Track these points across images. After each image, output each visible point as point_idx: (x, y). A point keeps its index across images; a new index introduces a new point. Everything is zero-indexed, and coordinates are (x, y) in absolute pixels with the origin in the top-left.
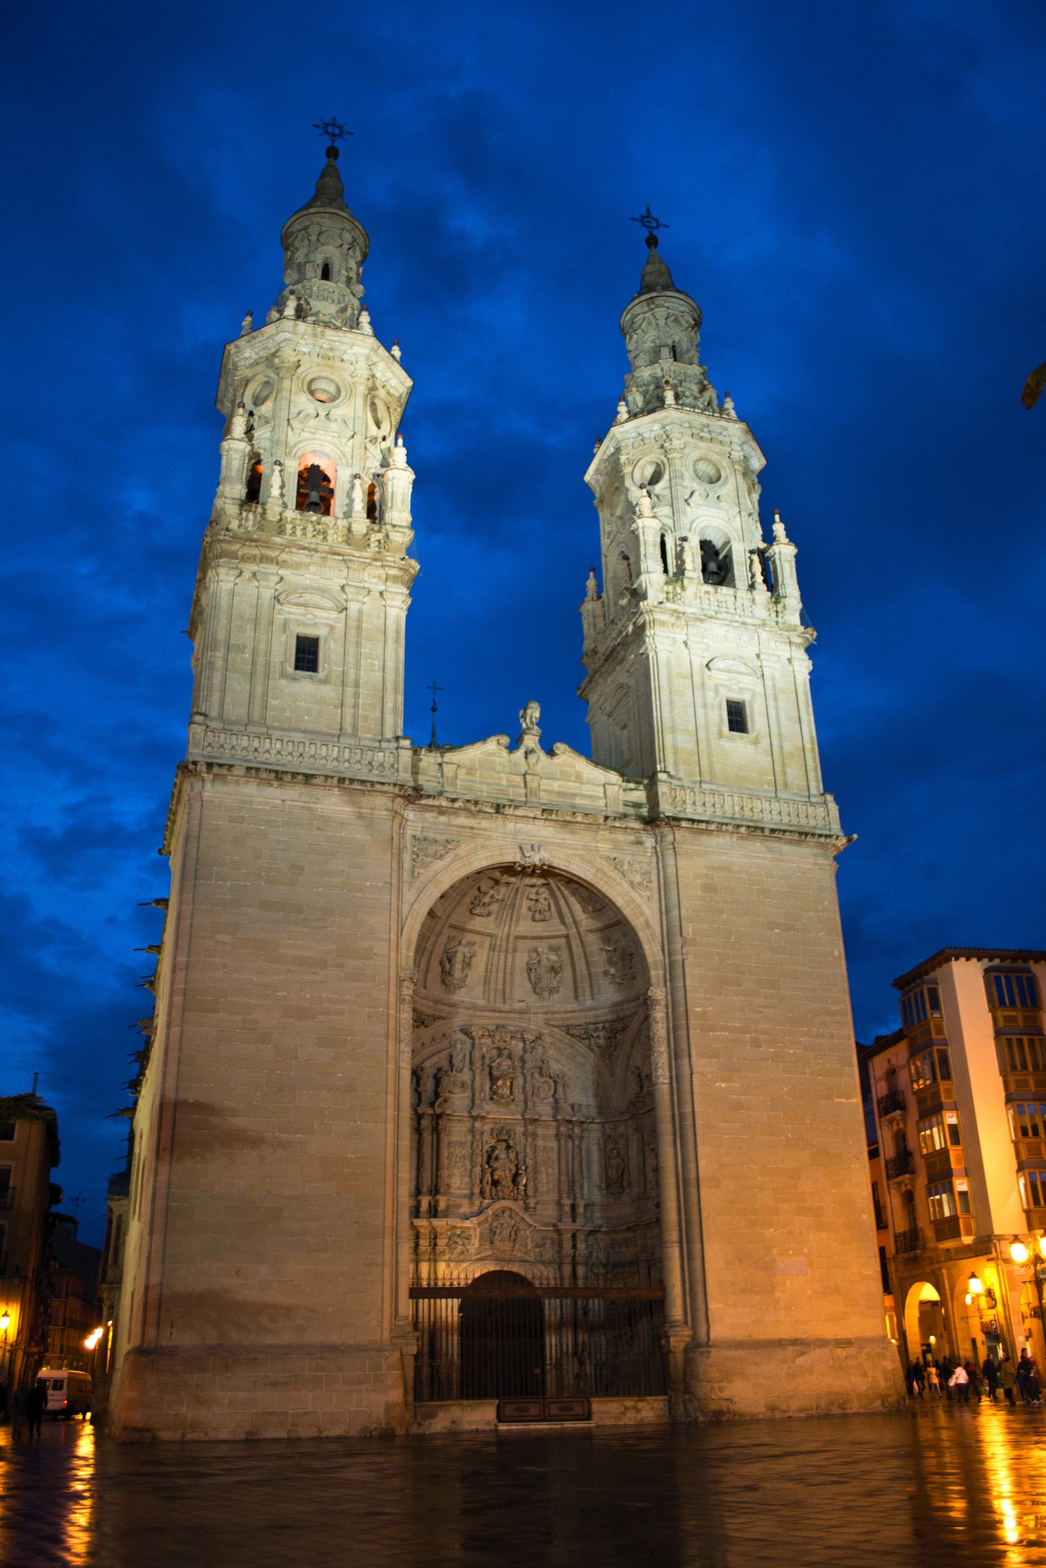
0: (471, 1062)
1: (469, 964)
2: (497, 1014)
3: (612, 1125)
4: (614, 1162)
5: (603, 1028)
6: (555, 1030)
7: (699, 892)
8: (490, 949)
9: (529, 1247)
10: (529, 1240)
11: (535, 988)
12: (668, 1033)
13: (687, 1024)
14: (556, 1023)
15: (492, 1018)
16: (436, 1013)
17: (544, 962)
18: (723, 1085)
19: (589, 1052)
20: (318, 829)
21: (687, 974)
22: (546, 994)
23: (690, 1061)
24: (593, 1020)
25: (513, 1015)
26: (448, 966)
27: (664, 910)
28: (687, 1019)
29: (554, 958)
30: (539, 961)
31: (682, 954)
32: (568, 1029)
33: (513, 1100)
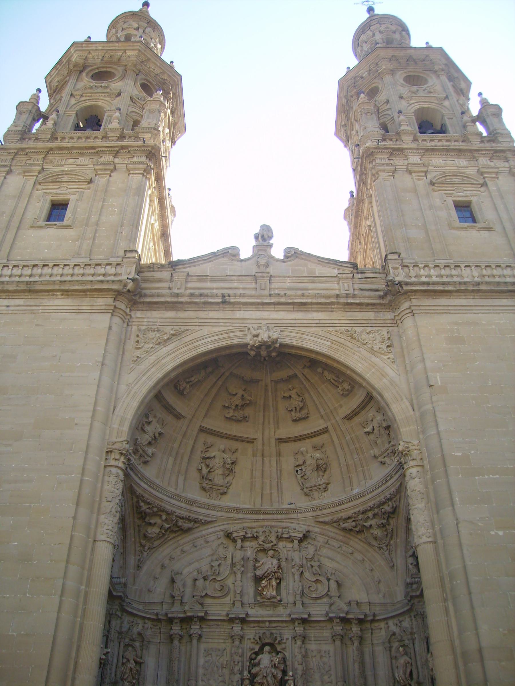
0: (233, 565)
1: (231, 471)
2: (262, 517)
3: (396, 621)
4: (402, 661)
5: (374, 515)
6: (327, 527)
7: (445, 345)
8: (253, 456)
11: (302, 490)
12: (427, 487)
13: (446, 471)
14: (326, 519)
15: (257, 520)
16: (191, 515)
17: (308, 462)
18: (501, 533)
19: (366, 546)
20: (37, 325)
21: (439, 420)
22: (316, 494)
23: (454, 509)
24: (361, 509)
25: (279, 516)
26: (205, 471)
27: (408, 368)
28: (445, 466)
29: (318, 455)
30: (304, 461)
31: (432, 403)
32: (335, 523)
33: (280, 601)
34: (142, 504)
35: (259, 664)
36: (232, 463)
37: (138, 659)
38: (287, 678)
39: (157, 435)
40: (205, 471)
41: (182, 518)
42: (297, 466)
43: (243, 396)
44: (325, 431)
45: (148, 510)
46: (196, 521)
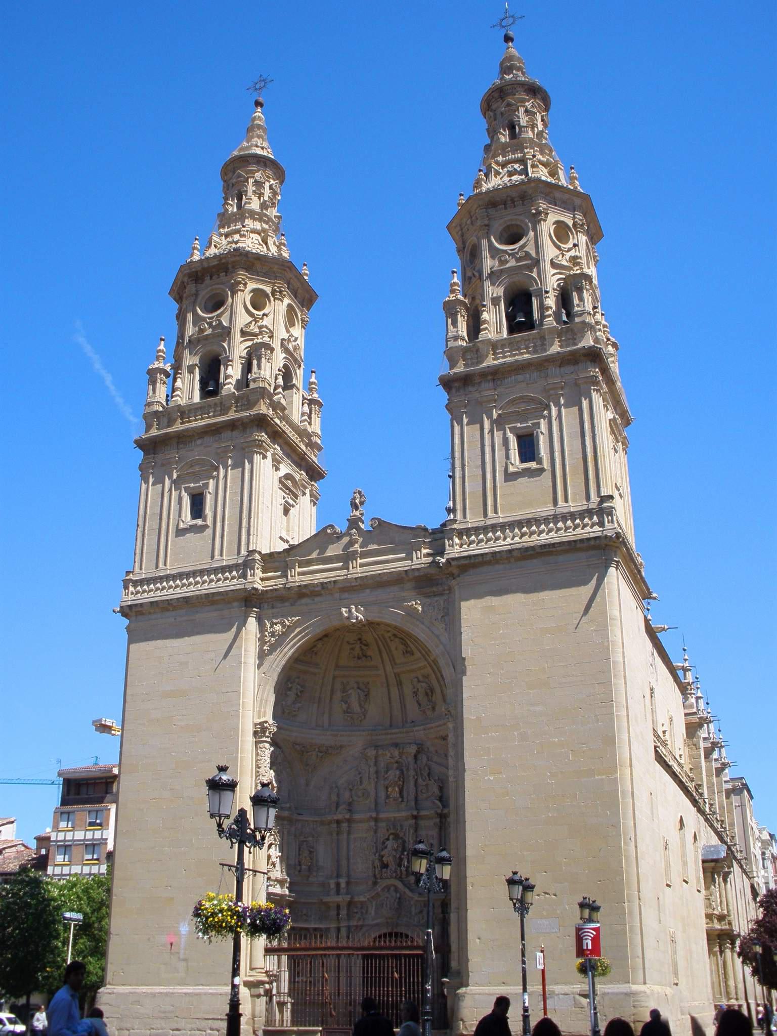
9: (413, 914)
10: (413, 909)
29: (424, 685)
34: (297, 746)
35: (386, 847)
36: (366, 695)
37: (311, 850)
38: (402, 857)
39: (299, 694)
40: (344, 706)
41: (331, 747)
42: (414, 692)
43: (361, 647)
44: (424, 667)
45: (303, 749)
46: (341, 747)
